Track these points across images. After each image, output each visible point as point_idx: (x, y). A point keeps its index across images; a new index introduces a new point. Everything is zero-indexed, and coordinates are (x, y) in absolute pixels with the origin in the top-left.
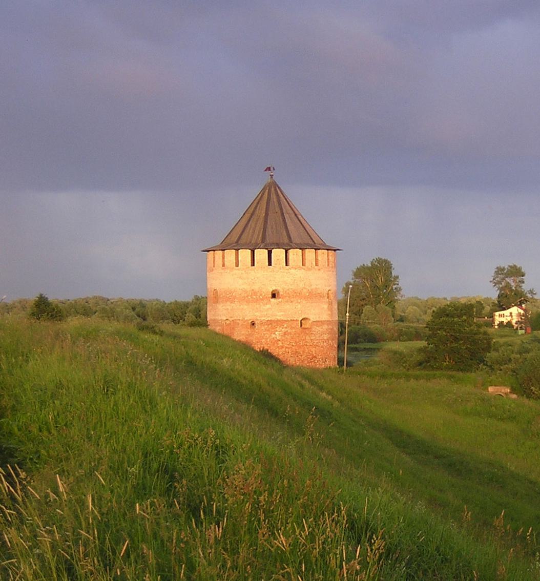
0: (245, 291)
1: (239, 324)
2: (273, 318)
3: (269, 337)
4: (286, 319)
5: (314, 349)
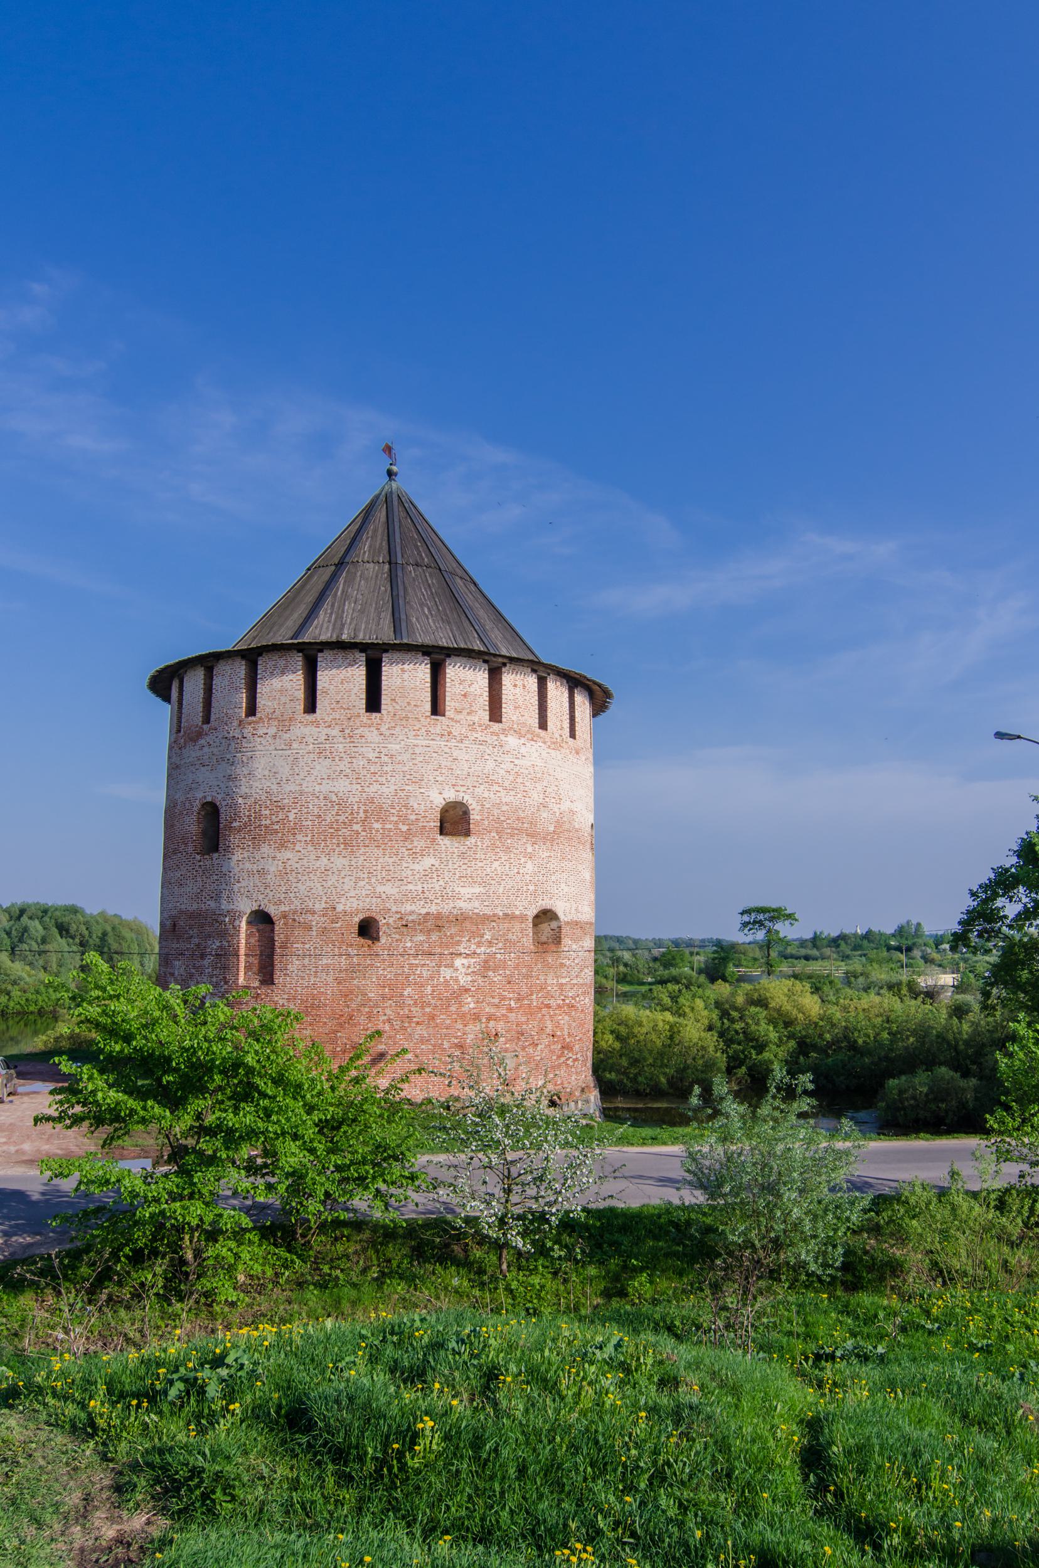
0: (342, 804)
1: (310, 928)
2: (446, 908)
3: (432, 978)
4: (488, 911)
5: (566, 1018)
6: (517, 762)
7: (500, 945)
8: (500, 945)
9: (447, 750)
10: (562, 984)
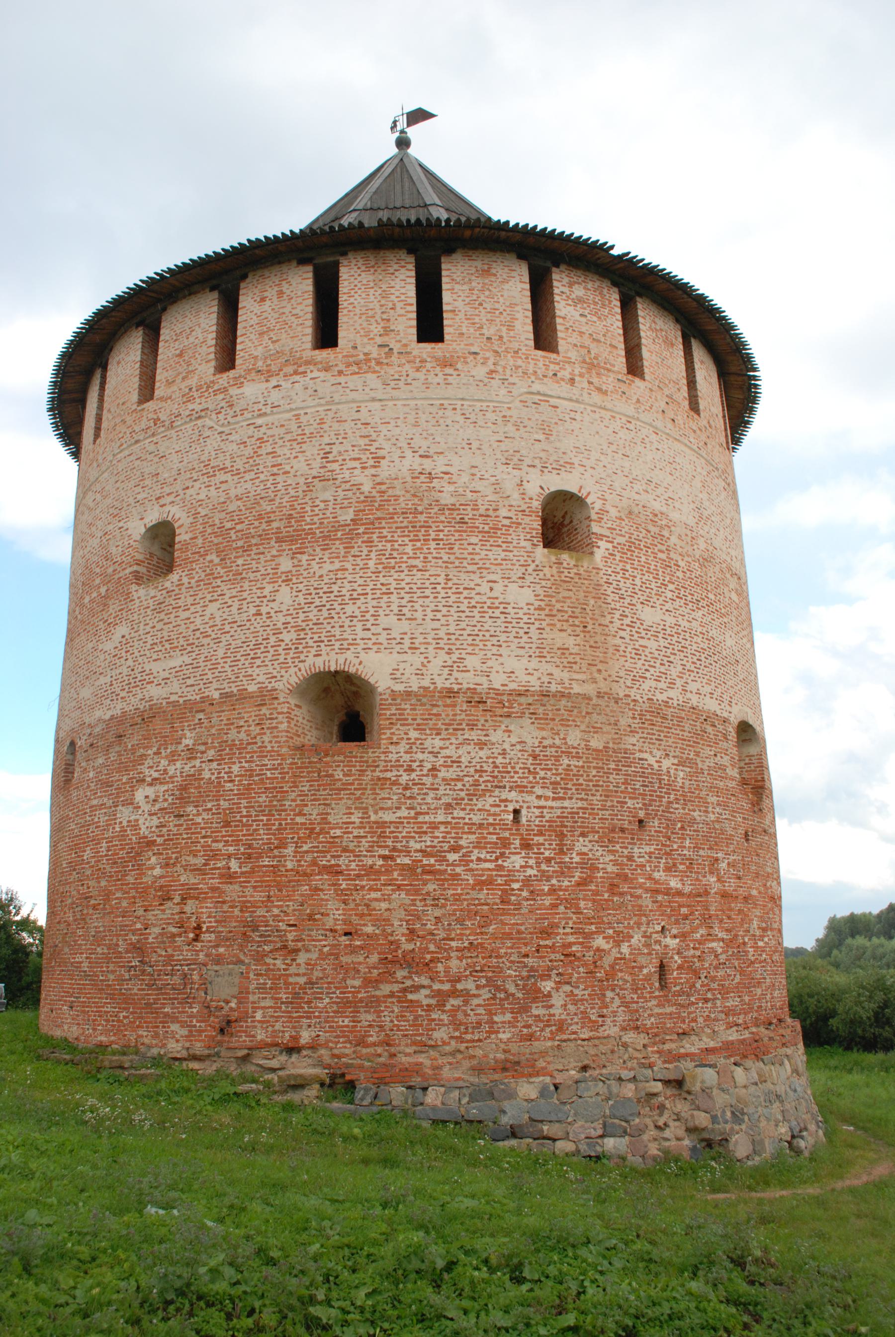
2: (133, 703)
6: (259, 421)
7: (211, 753)
8: (211, 753)
9: (152, 448)
10: (382, 824)
